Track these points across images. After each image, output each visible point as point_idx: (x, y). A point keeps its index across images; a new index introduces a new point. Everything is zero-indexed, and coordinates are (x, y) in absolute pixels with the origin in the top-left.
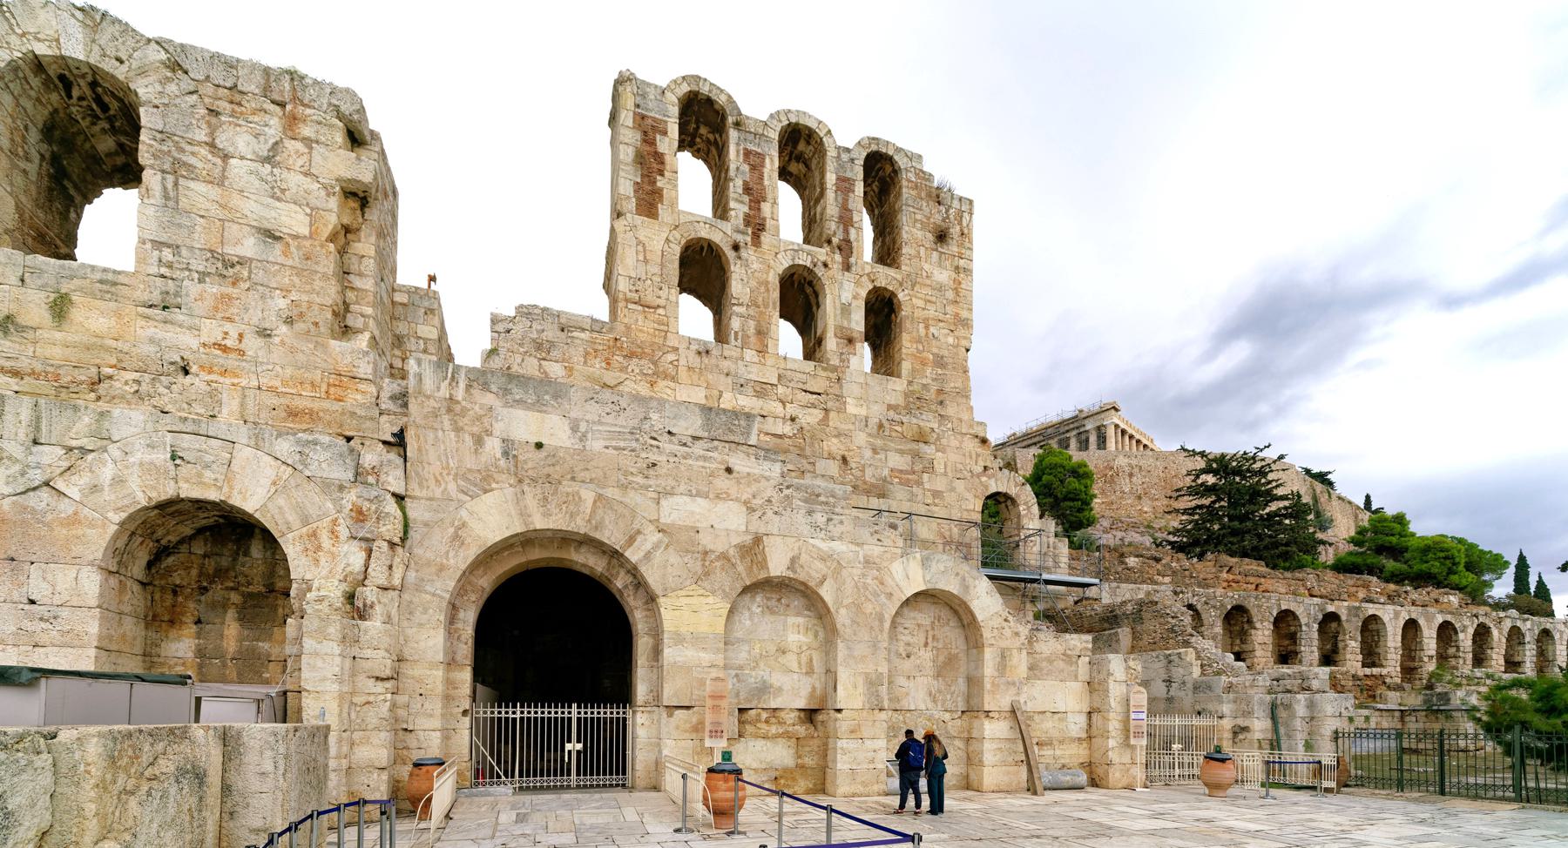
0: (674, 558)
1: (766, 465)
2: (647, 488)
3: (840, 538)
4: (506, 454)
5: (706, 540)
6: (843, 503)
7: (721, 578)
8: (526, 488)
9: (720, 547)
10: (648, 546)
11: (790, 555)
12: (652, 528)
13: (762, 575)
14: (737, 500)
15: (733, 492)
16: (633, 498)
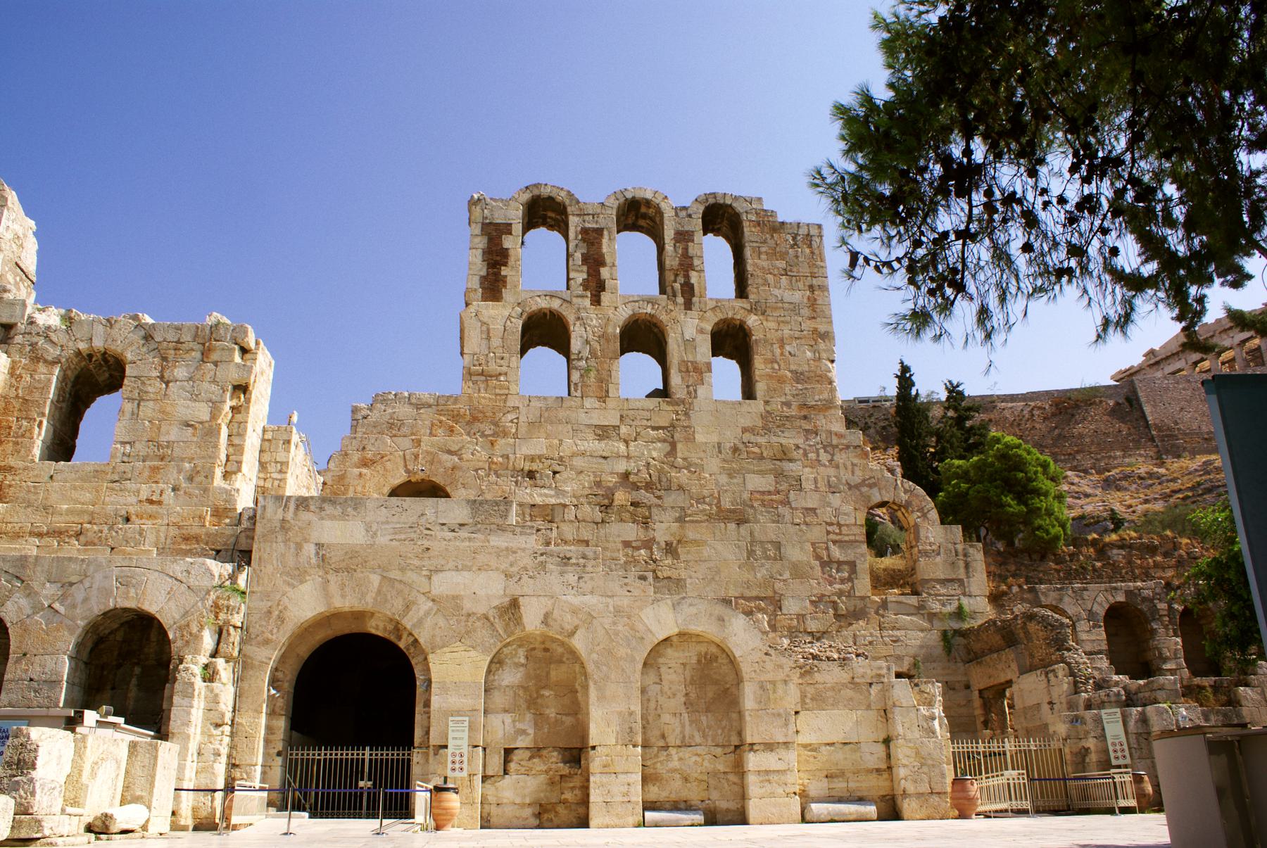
0: (442, 622)
1: (523, 538)
2: (420, 568)
3: (592, 593)
4: (318, 553)
5: (468, 605)
6: (593, 562)
7: (482, 634)
8: (329, 577)
9: (481, 609)
10: (421, 613)
11: (543, 612)
12: (423, 598)
13: (518, 633)
14: (497, 569)
15: (493, 563)
16: (411, 576)
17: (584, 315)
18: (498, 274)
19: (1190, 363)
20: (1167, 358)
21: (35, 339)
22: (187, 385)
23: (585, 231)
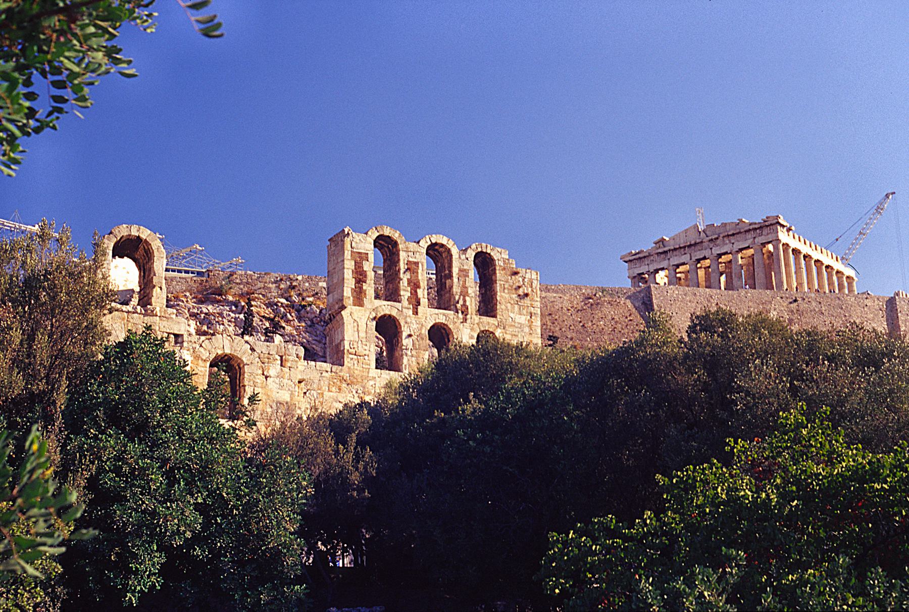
17: (408, 320)
18: (361, 288)
19: (694, 259)
20: (675, 249)
21: (194, 345)
22: (277, 381)
23: (409, 263)
